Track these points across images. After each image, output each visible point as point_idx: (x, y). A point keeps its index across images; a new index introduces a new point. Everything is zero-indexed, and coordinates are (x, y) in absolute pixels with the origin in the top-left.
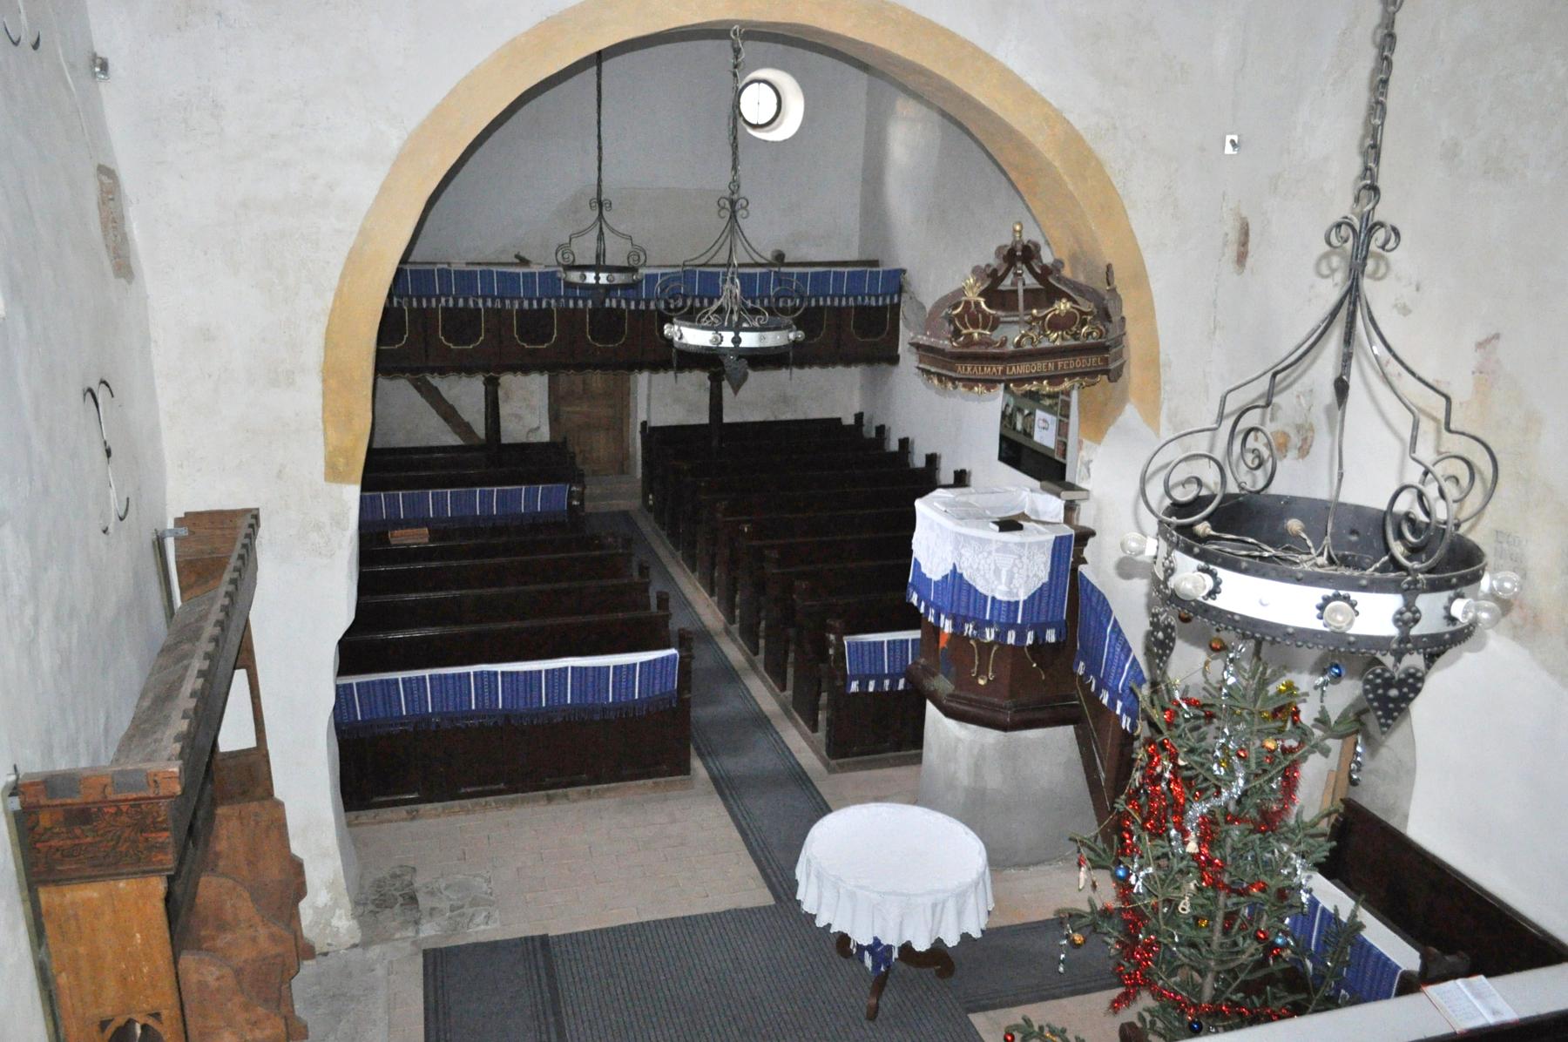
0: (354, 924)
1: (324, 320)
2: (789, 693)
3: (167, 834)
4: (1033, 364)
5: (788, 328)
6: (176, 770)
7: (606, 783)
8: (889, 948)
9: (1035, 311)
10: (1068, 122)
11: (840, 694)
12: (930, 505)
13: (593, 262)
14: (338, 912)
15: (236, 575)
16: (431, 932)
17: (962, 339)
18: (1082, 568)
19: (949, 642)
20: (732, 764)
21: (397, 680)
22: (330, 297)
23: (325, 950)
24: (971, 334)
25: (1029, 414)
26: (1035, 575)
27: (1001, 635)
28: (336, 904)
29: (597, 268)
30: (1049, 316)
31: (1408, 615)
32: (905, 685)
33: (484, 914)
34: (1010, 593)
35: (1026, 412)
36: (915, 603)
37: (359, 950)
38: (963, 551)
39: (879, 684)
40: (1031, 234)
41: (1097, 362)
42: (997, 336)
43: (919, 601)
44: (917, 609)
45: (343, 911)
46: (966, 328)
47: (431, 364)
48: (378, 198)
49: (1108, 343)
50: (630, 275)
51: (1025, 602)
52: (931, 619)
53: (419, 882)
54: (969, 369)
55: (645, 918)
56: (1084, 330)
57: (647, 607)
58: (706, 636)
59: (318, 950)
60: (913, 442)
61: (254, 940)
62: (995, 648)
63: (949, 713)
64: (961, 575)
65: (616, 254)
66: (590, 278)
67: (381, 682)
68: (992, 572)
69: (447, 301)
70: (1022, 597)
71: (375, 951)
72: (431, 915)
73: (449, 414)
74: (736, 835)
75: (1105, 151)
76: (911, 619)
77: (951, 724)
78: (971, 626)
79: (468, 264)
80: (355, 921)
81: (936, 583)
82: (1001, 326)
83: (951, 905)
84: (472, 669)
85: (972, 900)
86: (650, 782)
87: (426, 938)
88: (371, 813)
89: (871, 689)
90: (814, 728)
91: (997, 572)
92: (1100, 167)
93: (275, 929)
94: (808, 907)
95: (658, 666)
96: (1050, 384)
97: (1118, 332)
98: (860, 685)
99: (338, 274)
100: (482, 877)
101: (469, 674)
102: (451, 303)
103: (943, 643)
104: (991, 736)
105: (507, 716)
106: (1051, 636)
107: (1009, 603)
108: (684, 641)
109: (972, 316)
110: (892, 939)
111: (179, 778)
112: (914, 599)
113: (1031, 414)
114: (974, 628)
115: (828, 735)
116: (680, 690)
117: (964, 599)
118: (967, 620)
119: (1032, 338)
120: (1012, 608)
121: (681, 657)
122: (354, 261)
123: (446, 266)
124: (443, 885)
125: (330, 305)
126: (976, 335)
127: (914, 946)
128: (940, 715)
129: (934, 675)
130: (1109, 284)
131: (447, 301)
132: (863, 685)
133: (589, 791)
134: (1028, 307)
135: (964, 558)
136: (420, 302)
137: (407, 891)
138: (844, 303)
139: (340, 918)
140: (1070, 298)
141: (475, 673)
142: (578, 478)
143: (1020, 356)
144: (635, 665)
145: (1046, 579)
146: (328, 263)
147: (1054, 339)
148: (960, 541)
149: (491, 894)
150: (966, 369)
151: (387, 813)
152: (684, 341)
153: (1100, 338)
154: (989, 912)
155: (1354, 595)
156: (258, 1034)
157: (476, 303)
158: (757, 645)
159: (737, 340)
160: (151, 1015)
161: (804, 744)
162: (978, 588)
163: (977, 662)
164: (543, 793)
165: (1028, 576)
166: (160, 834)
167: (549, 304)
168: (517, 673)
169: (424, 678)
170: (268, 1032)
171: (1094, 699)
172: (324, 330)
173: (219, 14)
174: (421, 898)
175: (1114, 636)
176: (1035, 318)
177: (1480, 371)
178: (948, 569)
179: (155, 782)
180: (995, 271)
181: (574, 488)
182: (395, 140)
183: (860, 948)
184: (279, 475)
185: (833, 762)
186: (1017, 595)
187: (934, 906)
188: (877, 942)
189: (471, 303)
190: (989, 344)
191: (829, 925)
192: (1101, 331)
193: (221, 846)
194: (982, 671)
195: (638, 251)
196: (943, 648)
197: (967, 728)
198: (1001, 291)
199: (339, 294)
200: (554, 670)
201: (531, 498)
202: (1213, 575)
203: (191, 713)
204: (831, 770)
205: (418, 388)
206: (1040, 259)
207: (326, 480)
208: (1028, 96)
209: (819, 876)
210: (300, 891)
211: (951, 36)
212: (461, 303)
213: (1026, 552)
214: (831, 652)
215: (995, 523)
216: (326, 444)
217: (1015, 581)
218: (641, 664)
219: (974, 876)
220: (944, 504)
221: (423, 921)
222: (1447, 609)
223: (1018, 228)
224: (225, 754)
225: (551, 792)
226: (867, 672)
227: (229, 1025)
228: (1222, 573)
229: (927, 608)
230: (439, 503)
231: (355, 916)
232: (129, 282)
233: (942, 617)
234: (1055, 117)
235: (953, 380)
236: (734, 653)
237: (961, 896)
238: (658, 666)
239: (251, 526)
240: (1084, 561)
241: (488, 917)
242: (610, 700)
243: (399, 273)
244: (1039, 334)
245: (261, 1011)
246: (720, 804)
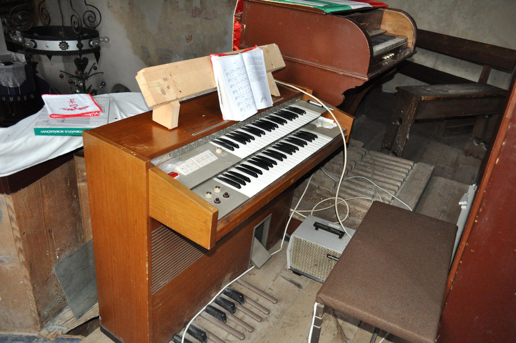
18: (37, 74)
25: (14, 33)
31: (80, 45)
35: (13, 32)
51: (20, 86)
78: (4, 98)
91: (8, 78)
106: (32, 96)
113: (15, 32)
114: (5, 98)
145: (25, 79)
155: (67, 42)
163: (10, 109)
177: (130, 4)
186: (17, 85)
202: (34, 42)
228: (36, 41)
240: (37, 72)
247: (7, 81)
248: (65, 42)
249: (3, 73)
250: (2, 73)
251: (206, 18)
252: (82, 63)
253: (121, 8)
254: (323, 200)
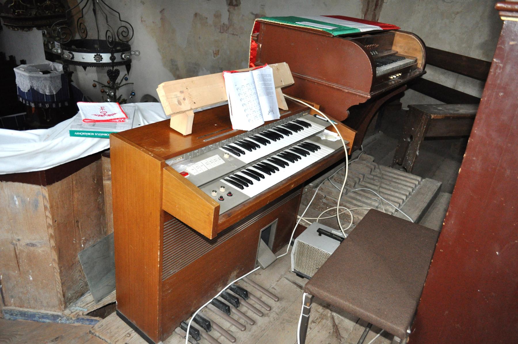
17: (16, 14)
18: (72, 83)
25: (52, 43)
26: (57, 86)
27: (51, 105)
31: (113, 58)
35: (52, 42)
36: (21, 101)
38: (33, 82)
43: (22, 100)
51: (56, 94)
52: (28, 105)
78: (41, 104)
81: (27, 93)
91: (45, 86)
106: (66, 104)
113: (54, 43)
114: (42, 105)
118: (39, 103)
126: (21, 12)
135: (33, 84)
145: (61, 87)
148: (31, 78)
155: (101, 54)
177: (161, 19)
186: (53, 92)
202: (72, 54)
213: (53, 80)
222: (121, 56)
228: (74, 53)
229: (25, 102)
233: (31, 103)
235: (16, 27)
240: (72, 81)
248: (99, 55)
249: (41, 81)
250: (40, 81)
251: (233, 34)
252: (114, 75)
253: (153, 22)
254: (329, 208)
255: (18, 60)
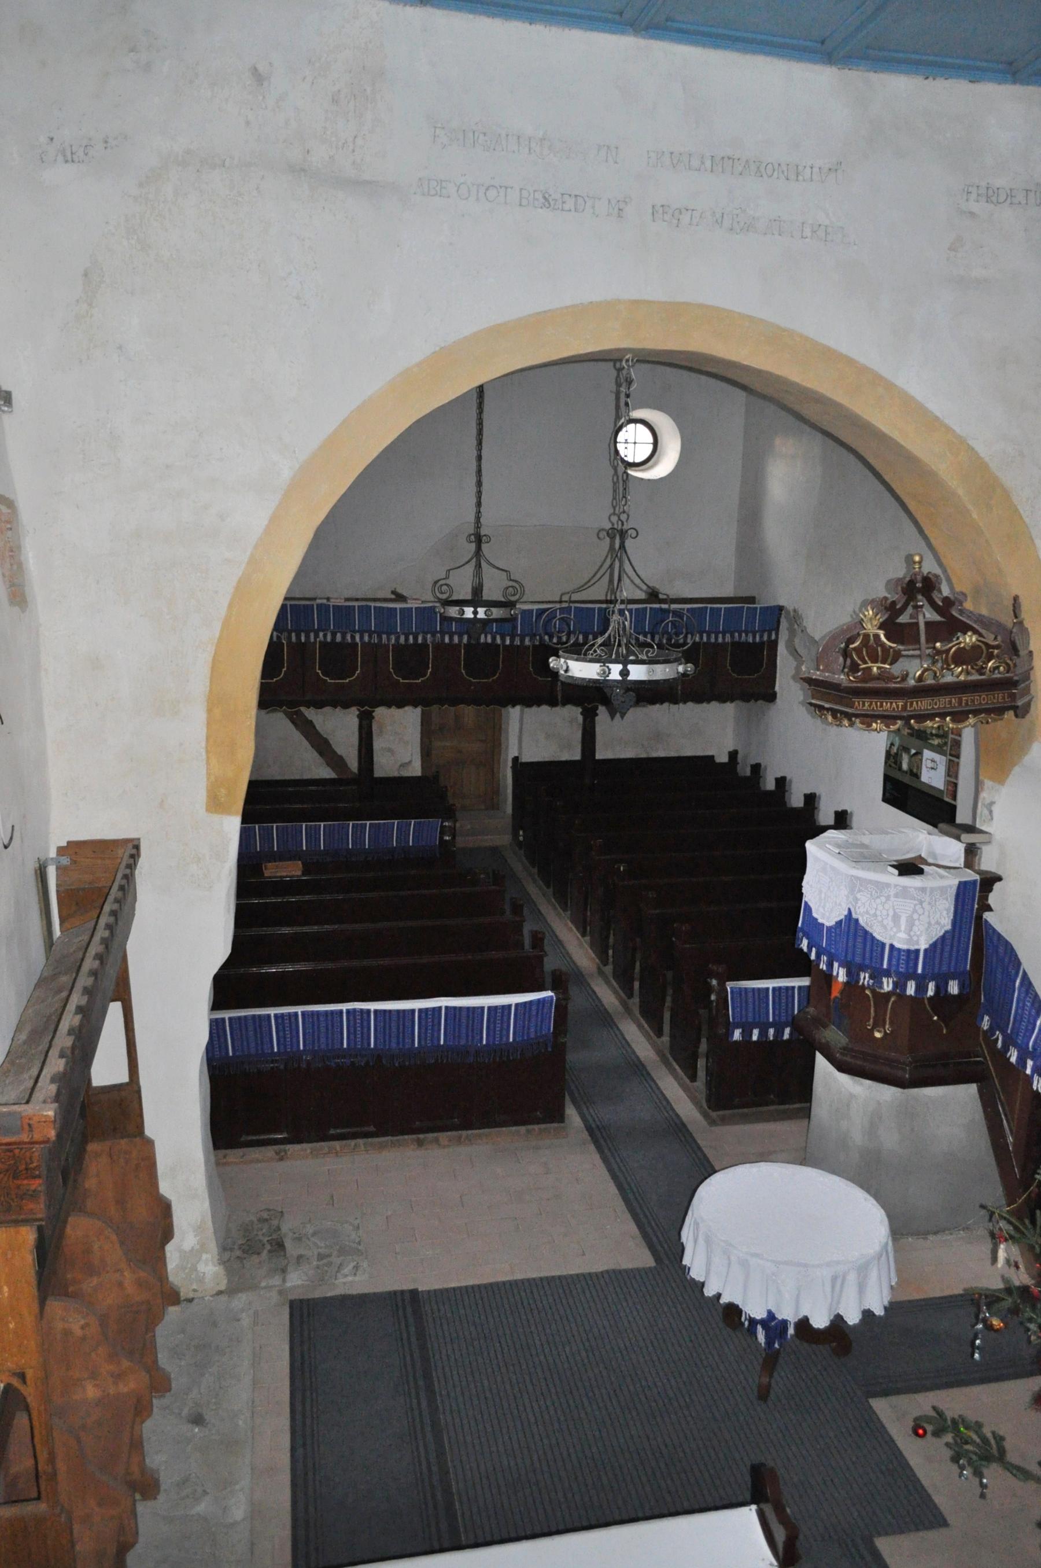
0: (219, 1270)
1: (211, 649)
2: (666, 1039)
3: (38, 1181)
4: (936, 699)
5: (677, 660)
6: (51, 1113)
7: (476, 1129)
8: (784, 1323)
9: (938, 645)
10: (973, 449)
11: (721, 1043)
12: (821, 847)
13: (469, 597)
14: (204, 1256)
15: (116, 906)
16: (297, 1281)
17: (860, 674)
18: (987, 916)
19: (842, 992)
20: (604, 1113)
21: (269, 1016)
22: (217, 626)
23: (191, 1295)
24: (870, 669)
25: (915, 754)
26: (938, 923)
27: (900, 985)
28: (203, 1248)
29: (476, 601)
30: (953, 649)
32: (791, 1034)
33: (352, 1264)
34: (909, 941)
35: (913, 751)
36: (805, 949)
37: (224, 1298)
38: (859, 896)
39: (763, 1033)
40: (929, 567)
41: (1004, 698)
42: (897, 669)
43: (810, 948)
44: (807, 956)
45: (209, 1256)
46: (865, 662)
47: (308, 697)
48: (267, 530)
49: (1016, 678)
50: (508, 609)
51: (926, 950)
52: (823, 966)
53: (286, 1227)
54: (867, 704)
55: (519, 1276)
56: (990, 664)
57: (520, 945)
58: (580, 977)
59: (183, 1295)
60: (791, 781)
61: (120, 1285)
62: (893, 999)
63: (842, 1067)
64: (857, 920)
65: (492, 591)
66: (469, 613)
67: (254, 1016)
68: (890, 918)
69: (325, 636)
70: (923, 946)
71: (241, 1300)
72: (298, 1263)
73: (322, 746)
74: (613, 1190)
75: (1009, 478)
76: (801, 965)
77: (844, 1079)
78: (867, 975)
79: (347, 600)
80: (222, 1267)
81: (829, 929)
82: (901, 660)
83: (852, 1277)
84: (344, 1007)
85: (874, 1275)
86: (523, 1129)
87: (295, 1287)
88: (239, 1152)
89: (755, 1038)
90: (693, 1078)
91: (896, 918)
92: (1006, 495)
93: (142, 1274)
94: (696, 1273)
95: (534, 1008)
96: (953, 721)
97: (1026, 668)
98: (743, 1034)
99: (226, 604)
100: (351, 1224)
101: (341, 1012)
102: (329, 639)
103: (835, 993)
104: (888, 1093)
105: (378, 1056)
106: (954, 988)
107: (908, 951)
108: (559, 982)
109: (872, 650)
110: (788, 1314)
111: (55, 1121)
112: (804, 945)
113: (919, 753)
114: (871, 977)
115: (708, 1084)
116: (556, 1034)
117: (859, 945)
118: (862, 968)
119: (935, 673)
120: (912, 956)
121: (557, 1000)
122: (243, 591)
123: (325, 601)
124: (311, 1231)
125: (217, 635)
126: (875, 669)
127: (811, 1322)
128: (831, 1068)
129: (825, 1026)
130: (1016, 617)
131: (325, 636)
132: (747, 1033)
133: (460, 1137)
134: (931, 639)
135: (859, 904)
136: (298, 637)
137: (275, 1236)
138: (720, 640)
139: (206, 1265)
140: (975, 632)
141: (348, 1011)
142: (450, 813)
143: (922, 691)
144: (510, 1006)
145: (949, 927)
146: (216, 592)
147: (958, 674)
148: (855, 885)
149: (359, 1243)
150: (864, 705)
151: (255, 1153)
152: (570, 674)
153: (1008, 672)
154: (892, 1287)
156: (123, 1389)
157: (353, 638)
158: (632, 989)
159: (625, 673)
160: (14, 1374)
161: (681, 1093)
162: (875, 935)
164: (414, 1136)
165: (929, 923)
166: (32, 1182)
167: (425, 639)
168: (390, 1011)
169: (296, 1014)
170: (132, 1385)
171: (1001, 1056)
172: (210, 659)
173: (120, 348)
174: (288, 1244)
175: (1023, 989)
176: (939, 652)
178: (840, 915)
179: (29, 1125)
180: (894, 603)
181: (447, 824)
182: (286, 471)
183: (753, 1322)
184: (162, 804)
185: (714, 1114)
186: (917, 943)
187: (834, 1279)
188: (771, 1315)
189: (349, 638)
190: (891, 678)
191: (719, 1296)
192: (1007, 664)
193: (90, 1183)
194: (879, 1024)
195: (516, 586)
196: (836, 997)
197: (862, 1084)
198: (901, 624)
199: (226, 623)
200: (427, 1010)
201: (403, 832)
203: (69, 1052)
204: (712, 1123)
205: (293, 722)
206: (940, 591)
207: (207, 810)
208: (932, 423)
209: (708, 1242)
210: (167, 1234)
211: (850, 362)
212: (339, 638)
213: (927, 899)
214: (713, 997)
215: (893, 866)
216: (209, 774)
217: (915, 929)
218: (517, 1005)
219: (877, 1248)
220: (838, 846)
221: (289, 1269)
223: (917, 558)
224: (96, 1088)
225: (421, 1136)
226: (750, 1020)
227: (94, 1376)
229: (818, 956)
230: (313, 835)
231: (223, 1262)
232: (23, 611)
233: (836, 965)
234: (958, 444)
235: (849, 716)
236: (607, 996)
237: (862, 1270)
238: (534, 1008)
239: (132, 856)
240: (989, 909)
241: (356, 1268)
242: (484, 1042)
243: (283, 607)
244: (942, 669)
245: (126, 1364)
246: (597, 1158)
247: (891, 924)
249: (888, 898)
250: (883, 899)
255: (825, 815)
